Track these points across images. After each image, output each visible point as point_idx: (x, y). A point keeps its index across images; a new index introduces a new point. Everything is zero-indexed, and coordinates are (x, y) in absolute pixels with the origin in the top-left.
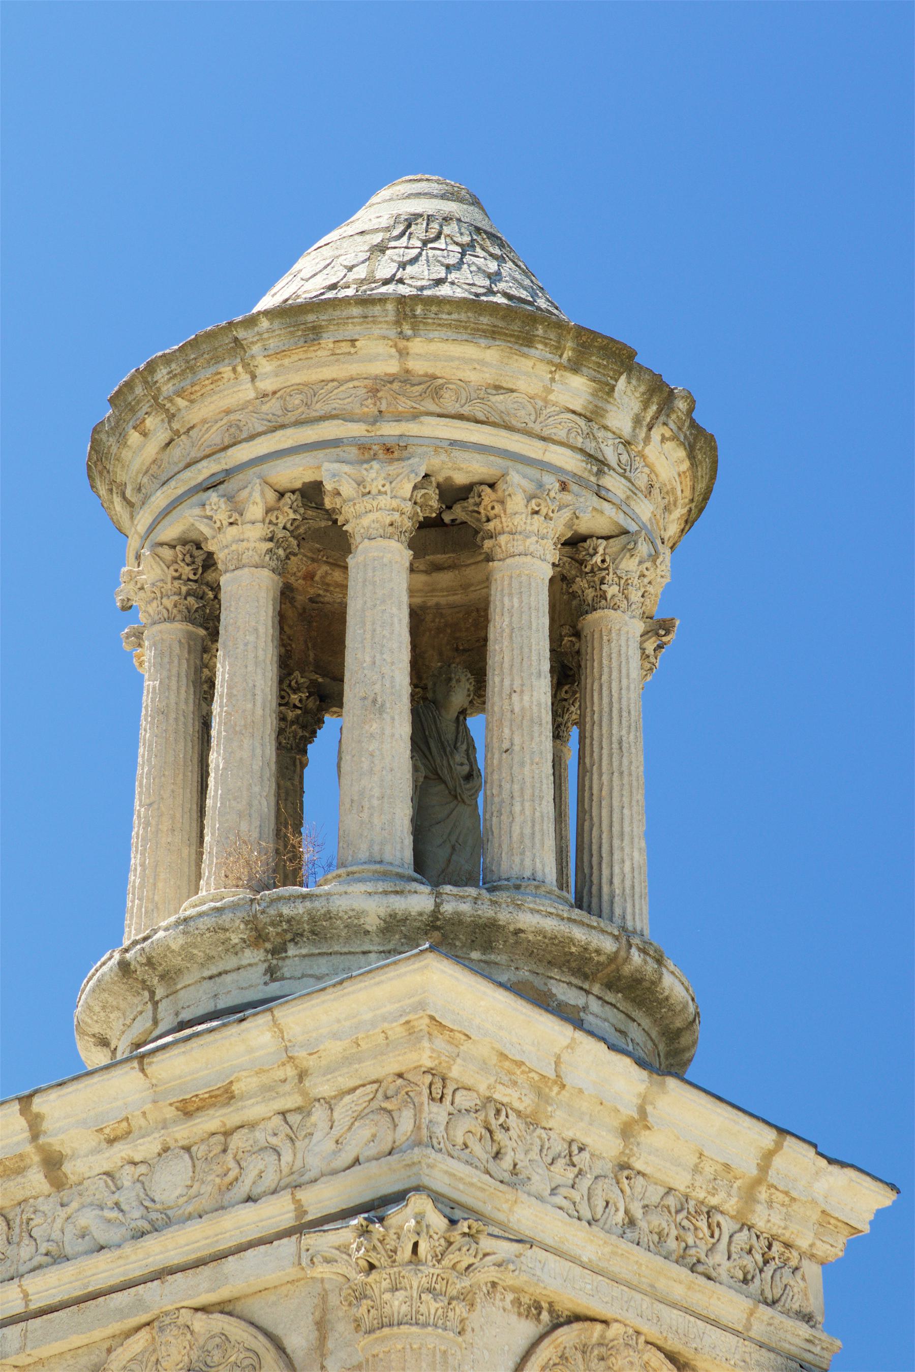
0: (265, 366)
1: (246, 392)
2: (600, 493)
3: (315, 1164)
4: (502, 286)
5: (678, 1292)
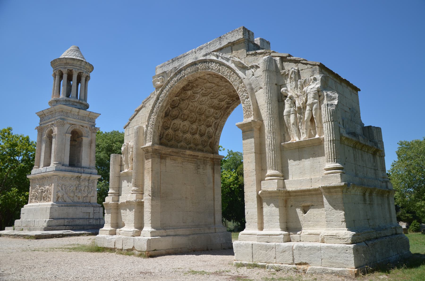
0: (58, 62)
1: (57, 63)
2: (81, 70)
3: (56, 116)
4: (76, 55)
5: (82, 122)
